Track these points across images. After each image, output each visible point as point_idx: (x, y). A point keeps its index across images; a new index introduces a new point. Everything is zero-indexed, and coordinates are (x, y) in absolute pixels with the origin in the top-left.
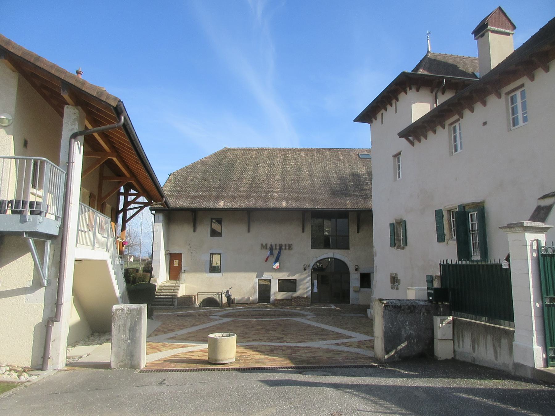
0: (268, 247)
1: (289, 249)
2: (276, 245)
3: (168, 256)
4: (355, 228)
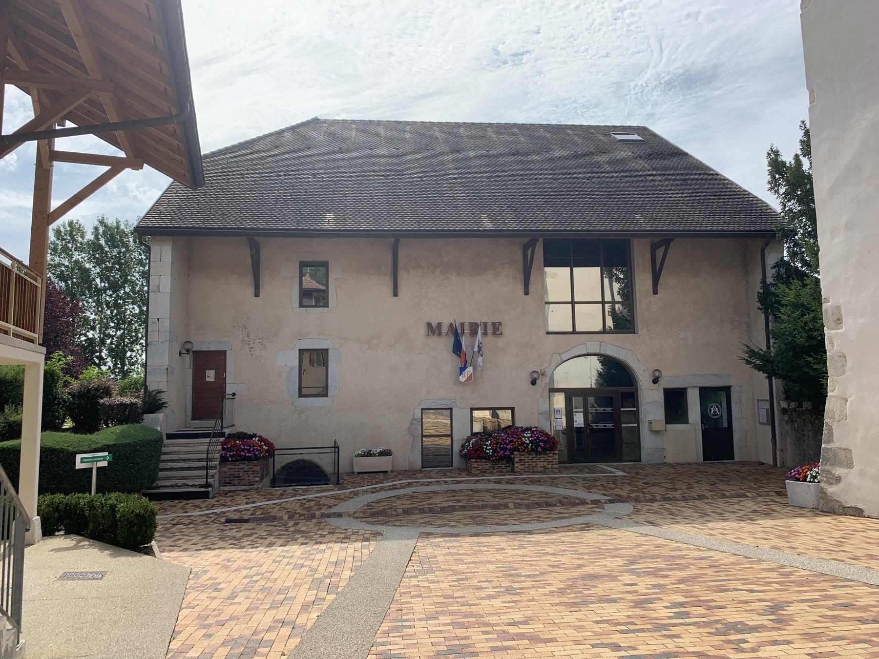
0: (445, 329)
1: (494, 334)
2: (462, 324)
3: (188, 359)
4: (649, 281)
